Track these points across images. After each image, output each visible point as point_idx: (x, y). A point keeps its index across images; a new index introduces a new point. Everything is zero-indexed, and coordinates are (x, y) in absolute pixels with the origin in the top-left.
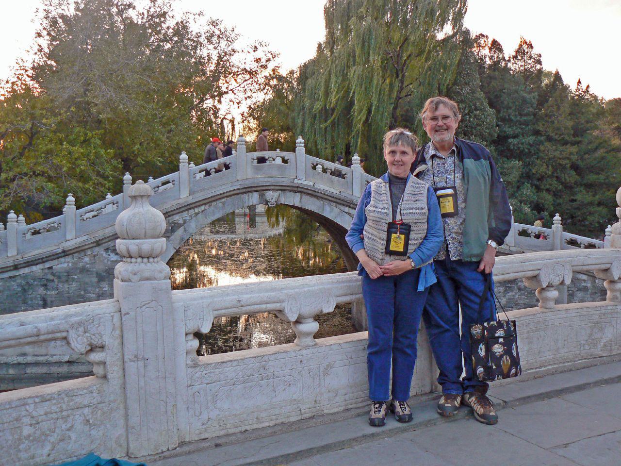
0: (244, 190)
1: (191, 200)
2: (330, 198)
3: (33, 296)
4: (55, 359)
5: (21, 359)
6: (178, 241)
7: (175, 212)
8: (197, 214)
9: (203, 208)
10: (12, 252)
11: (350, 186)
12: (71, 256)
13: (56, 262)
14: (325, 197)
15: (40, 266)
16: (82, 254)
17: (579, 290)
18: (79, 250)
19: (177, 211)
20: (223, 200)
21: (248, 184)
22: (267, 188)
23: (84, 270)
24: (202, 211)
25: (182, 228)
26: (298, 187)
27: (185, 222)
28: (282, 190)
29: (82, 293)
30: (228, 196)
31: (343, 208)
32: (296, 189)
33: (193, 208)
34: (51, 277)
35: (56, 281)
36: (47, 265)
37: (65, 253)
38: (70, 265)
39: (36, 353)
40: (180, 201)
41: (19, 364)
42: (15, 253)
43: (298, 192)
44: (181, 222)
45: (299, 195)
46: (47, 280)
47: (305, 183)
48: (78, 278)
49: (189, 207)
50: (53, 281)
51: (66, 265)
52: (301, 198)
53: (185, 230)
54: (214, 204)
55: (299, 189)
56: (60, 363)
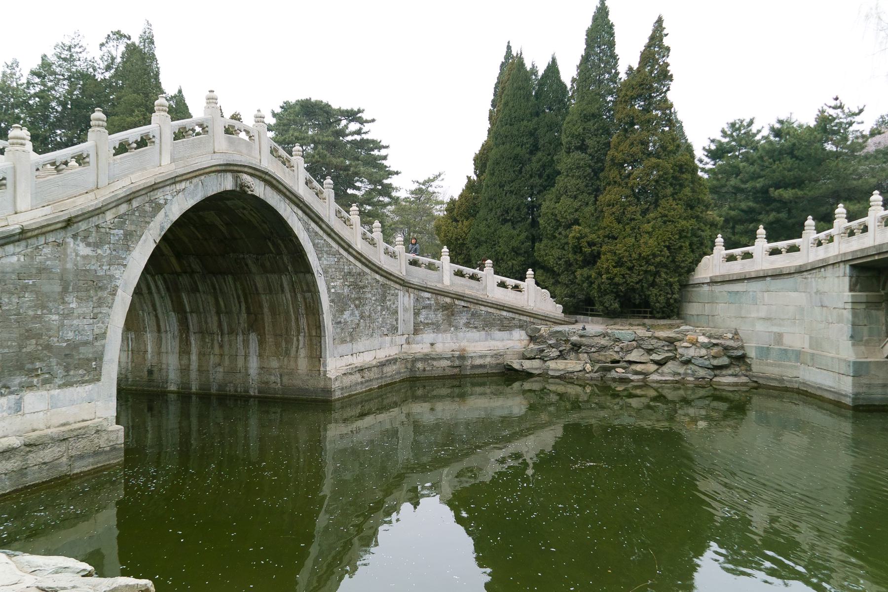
0: (224, 168)
2: (288, 193)
8: (178, 192)
12: (23, 243)
14: (285, 190)
16: (42, 240)
17: (424, 308)
18: (42, 231)
20: (203, 177)
23: (42, 270)
25: (162, 212)
26: (266, 173)
27: (166, 203)
29: (39, 312)
30: (207, 173)
33: (175, 183)
37: (22, 235)
38: (22, 259)
44: (162, 202)
48: (34, 284)
49: (174, 180)
51: (15, 258)
54: (195, 181)
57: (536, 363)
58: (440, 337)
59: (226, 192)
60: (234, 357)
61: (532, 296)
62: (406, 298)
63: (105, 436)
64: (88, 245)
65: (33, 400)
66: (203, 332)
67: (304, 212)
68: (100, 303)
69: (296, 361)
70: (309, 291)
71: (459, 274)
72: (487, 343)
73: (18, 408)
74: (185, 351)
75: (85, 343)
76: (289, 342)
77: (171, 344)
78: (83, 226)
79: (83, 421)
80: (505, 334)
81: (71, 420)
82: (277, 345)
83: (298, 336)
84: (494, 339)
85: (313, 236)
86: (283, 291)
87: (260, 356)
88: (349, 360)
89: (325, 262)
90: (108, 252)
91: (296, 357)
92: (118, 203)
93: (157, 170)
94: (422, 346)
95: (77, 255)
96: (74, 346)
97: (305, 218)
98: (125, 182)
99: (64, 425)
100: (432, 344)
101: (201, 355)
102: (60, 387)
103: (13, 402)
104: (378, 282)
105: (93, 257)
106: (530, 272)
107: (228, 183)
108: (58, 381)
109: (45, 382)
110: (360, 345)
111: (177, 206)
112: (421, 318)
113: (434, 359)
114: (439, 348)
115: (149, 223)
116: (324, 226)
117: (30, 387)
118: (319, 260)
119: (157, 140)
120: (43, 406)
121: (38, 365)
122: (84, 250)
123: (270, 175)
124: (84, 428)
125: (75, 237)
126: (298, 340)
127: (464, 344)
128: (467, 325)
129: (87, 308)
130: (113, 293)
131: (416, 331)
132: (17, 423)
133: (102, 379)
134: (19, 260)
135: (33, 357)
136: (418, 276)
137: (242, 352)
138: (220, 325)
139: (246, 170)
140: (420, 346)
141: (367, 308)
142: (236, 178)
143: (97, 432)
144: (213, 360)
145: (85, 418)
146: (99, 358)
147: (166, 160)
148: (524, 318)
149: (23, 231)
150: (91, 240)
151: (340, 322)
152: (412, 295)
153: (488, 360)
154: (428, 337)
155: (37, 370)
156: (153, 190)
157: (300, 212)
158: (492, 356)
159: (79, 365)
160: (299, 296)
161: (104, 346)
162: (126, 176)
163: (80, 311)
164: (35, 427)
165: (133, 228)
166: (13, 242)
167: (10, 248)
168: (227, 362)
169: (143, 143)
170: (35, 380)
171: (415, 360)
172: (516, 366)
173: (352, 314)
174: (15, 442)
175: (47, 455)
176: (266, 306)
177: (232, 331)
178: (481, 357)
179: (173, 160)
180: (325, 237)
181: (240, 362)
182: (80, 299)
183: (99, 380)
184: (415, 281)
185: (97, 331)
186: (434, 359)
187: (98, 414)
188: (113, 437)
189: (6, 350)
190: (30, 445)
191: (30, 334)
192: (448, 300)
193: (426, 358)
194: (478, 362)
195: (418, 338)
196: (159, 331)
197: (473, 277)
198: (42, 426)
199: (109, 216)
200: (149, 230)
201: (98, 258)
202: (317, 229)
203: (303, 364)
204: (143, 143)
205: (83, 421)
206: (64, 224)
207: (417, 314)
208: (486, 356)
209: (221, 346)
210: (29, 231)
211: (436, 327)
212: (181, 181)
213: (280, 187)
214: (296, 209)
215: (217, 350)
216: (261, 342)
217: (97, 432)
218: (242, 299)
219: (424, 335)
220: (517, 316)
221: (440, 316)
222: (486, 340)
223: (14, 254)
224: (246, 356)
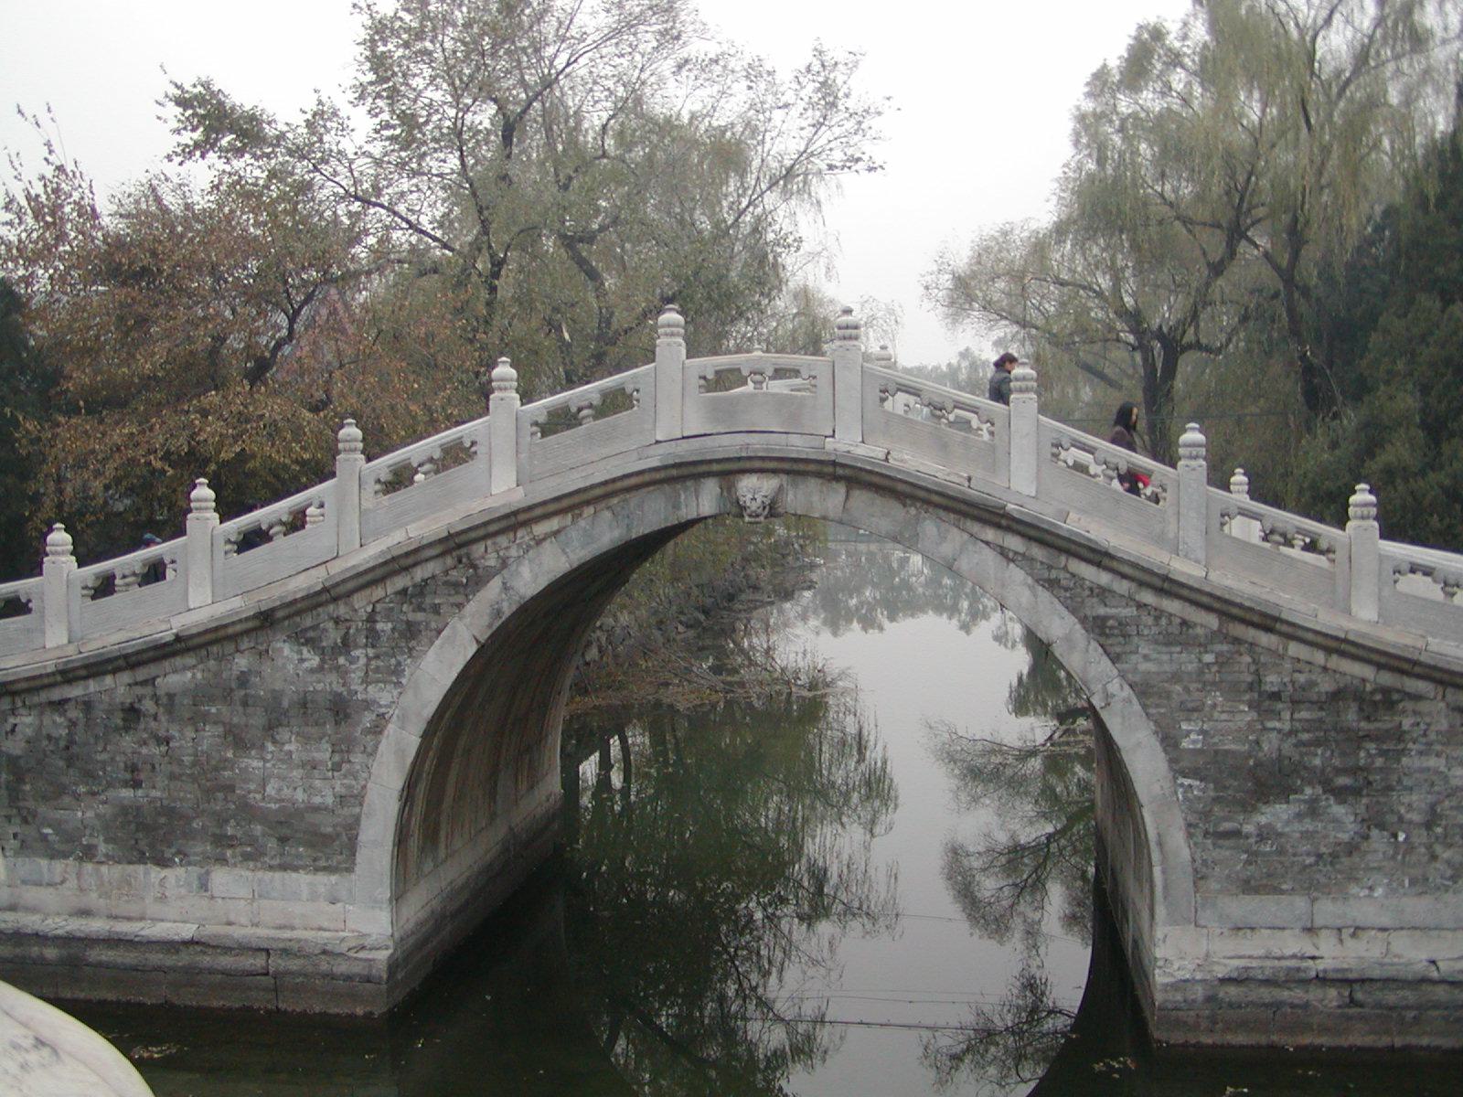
1: (519, 498)
3: (104, 756)
6: (485, 620)
7: (473, 535)
9: (554, 524)
11: (995, 456)
16: (230, 647)
19: (481, 532)
20: (615, 501)
21: (686, 451)
24: (556, 533)
25: (496, 583)
26: (834, 463)
28: (787, 472)
31: (976, 528)
32: (830, 469)
35: (163, 718)
36: (142, 674)
37: (181, 646)
38: (199, 676)
40: (490, 503)
43: (837, 478)
45: (841, 489)
47: (861, 451)
49: (514, 521)
52: (847, 497)
53: (506, 588)
55: (840, 471)
65: (221, 878)
73: (204, 885)
79: (320, 929)
81: (297, 922)
88: (1292, 944)
89: (1144, 666)
97: (1038, 552)
109: (247, 857)
115: (460, 606)
117: (222, 861)
118: (1115, 659)
130: (377, 729)
145: (325, 925)
151: (1236, 834)
157: (1014, 543)
182: (306, 739)
183: (350, 870)
187: (350, 925)
198: (243, 920)
200: (460, 619)
202: (1104, 578)
214: (990, 534)
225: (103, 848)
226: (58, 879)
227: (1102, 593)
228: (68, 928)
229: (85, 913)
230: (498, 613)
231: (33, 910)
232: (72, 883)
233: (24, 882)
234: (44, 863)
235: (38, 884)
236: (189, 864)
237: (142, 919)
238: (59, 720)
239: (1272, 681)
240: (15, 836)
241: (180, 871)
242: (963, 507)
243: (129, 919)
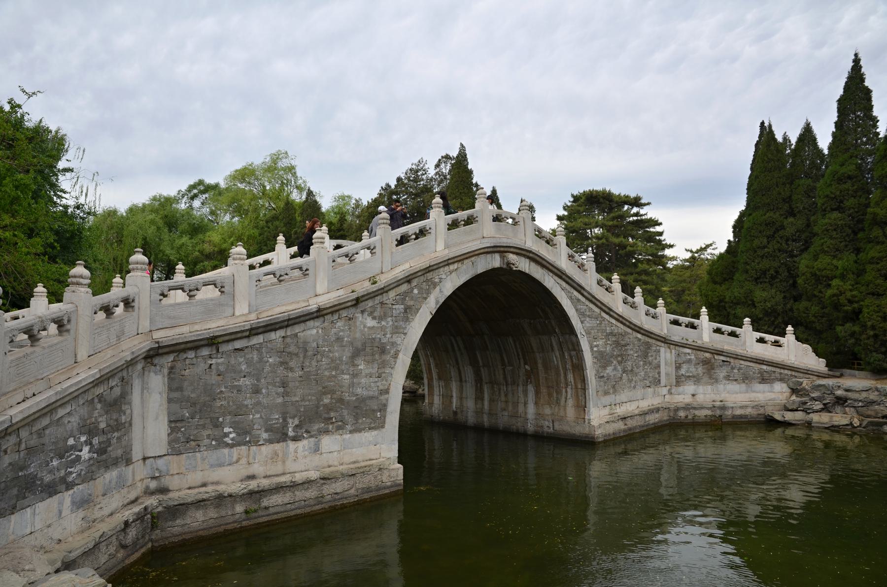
4: (299, 478)
5: (253, 485)
8: (451, 272)
9: (456, 266)
10: (242, 308)
12: (322, 319)
13: (302, 326)
15: (281, 333)
16: (336, 316)
18: (335, 310)
20: (473, 259)
22: (506, 249)
25: (438, 288)
26: (530, 252)
29: (334, 373)
33: (448, 265)
34: (292, 349)
36: (289, 331)
37: (320, 313)
38: (320, 331)
39: (268, 474)
40: (437, 254)
41: (251, 493)
42: (246, 311)
46: (290, 354)
49: (448, 262)
50: (297, 355)
51: (315, 331)
53: (441, 291)
54: (466, 262)
56: (308, 483)
57: (799, 416)
58: (701, 389)
59: (494, 270)
60: (516, 404)
61: (793, 350)
62: (668, 355)
63: (386, 473)
64: (374, 318)
65: (328, 442)
66: (492, 383)
67: (567, 283)
68: (383, 364)
69: (565, 409)
70: (574, 350)
71: (718, 331)
72: (747, 395)
73: (316, 449)
74: (479, 398)
75: (372, 398)
76: (559, 392)
77: (470, 391)
78: (370, 303)
79: (370, 460)
80: (765, 387)
81: (360, 459)
82: (550, 395)
83: (566, 388)
84: (754, 392)
85: (575, 302)
86: (553, 350)
87: (536, 403)
89: (588, 325)
90: (391, 323)
91: (565, 407)
92: (398, 283)
93: (433, 255)
94: (685, 395)
95: (365, 326)
96: (363, 400)
97: (568, 287)
98: (406, 266)
99: (354, 462)
100: (693, 395)
101: (491, 401)
102: (351, 432)
103: (313, 443)
104: (640, 340)
105: (378, 328)
106: (790, 328)
107: (496, 262)
108: (349, 427)
109: (339, 428)
110: (623, 396)
111: (450, 283)
112: (683, 371)
113: (695, 408)
114: (700, 398)
115: (426, 298)
116: (585, 294)
117: (327, 432)
118: (582, 322)
119: (433, 231)
120: (336, 447)
121: (332, 414)
122: (370, 323)
123: (533, 253)
124: (369, 466)
125: (363, 312)
126: (566, 392)
127: (724, 396)
128: (727, 378)
129: (374, 369)
130: (396, 356)
131: (678, 383)
132: (317, 460)
133: (386, 426)
134: (318, 332)
135: (328, 408)
136: (680, 333)
137: (522, 400)
138: (505, 378)
139: (512, 250)
140: (683, 396)
141: (630, 363)
142: (502, 257)
143: (380, 469)
144: (500, 405)
145: (373, 457)
146: (383, 408)
147: (440, 246)
148: (786, 372)
149: (319, 310)
150: (376, 314)
151: (603, 377)
152: (673, 351)
153: (748, 411)
154: (689, 388)
155: (332, 418)
156: (429, 271)
157: (564, 284)
158: (753, 407)
159: (366, 414)
160: (566, 354)
161: (387, 400)
162: (407, 261)
163: (367, 371)
164: (330, 463)
165: (412, 303)
166: (313, 319)
167: (311, 323)
168: (510, 408)
169: (422, 233)
170: (331, 427)
171: (677, 409)
172: (778, 417)
173: (615, 369)
174: (314, 475)
175: (338, 487)
176: (540, 361)
177: (514, 383)
178: (741, 407)
179: (447, 246)
180: (587, 303)
181: (521, 408)
184: (676, 338)
185: (381, 387)
186: (695, 408)
187: (382, 455)
188: (393, 474)
189: (307, 403)
190: (324, 479)
191: (326, 391)
192: (708, 355)
193: (687, 407)
194: (738, 412)
195: (681, 389)
196: (461, 381)
197: (733, 334)
198: (336, 463)
199: (392, 294)
201: (383, 328)
202: (580, 297)
203: (571, 412)
204: (422, 233)
205: (370, 460)
206: (354, 302)
207: (678, 368)
208: (747, 407)
209: (506, 395)
210: (325, 309)
211: (697, 380)
212: (454, 263)
213: (544, 262)
214: (559, 281)
215: (503, 398)
216: (537, 393)
217: (380, 469)
218: (521, 356)
219: (686, 387)
220: (778, 370)
221: (700, 370)
222: (747, 392)
223: (314, 328)
224: (526, 404)
225: (265, 436)
226: (235, 459)
227: (579, 300)
228: (251, 487)
229: (252, 477)
230: (437, 302)
231: (217, 483)
232: (244, 461)
233: (212, 466)
234: (226, 451)
235: (221, 465)
236: (311, 436)
237: (284, 474)
238: (241, 360)
239: (608, 330)
240: (208, 436)
241: (305, 442)
242: (556, 271)
243: (277, 475)
